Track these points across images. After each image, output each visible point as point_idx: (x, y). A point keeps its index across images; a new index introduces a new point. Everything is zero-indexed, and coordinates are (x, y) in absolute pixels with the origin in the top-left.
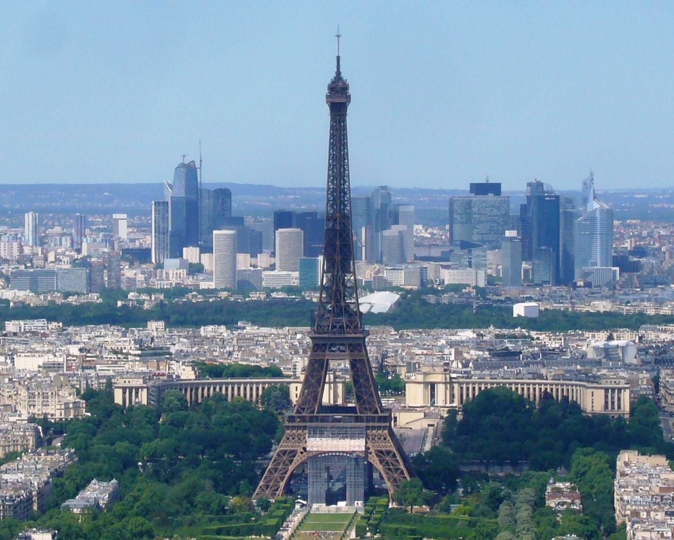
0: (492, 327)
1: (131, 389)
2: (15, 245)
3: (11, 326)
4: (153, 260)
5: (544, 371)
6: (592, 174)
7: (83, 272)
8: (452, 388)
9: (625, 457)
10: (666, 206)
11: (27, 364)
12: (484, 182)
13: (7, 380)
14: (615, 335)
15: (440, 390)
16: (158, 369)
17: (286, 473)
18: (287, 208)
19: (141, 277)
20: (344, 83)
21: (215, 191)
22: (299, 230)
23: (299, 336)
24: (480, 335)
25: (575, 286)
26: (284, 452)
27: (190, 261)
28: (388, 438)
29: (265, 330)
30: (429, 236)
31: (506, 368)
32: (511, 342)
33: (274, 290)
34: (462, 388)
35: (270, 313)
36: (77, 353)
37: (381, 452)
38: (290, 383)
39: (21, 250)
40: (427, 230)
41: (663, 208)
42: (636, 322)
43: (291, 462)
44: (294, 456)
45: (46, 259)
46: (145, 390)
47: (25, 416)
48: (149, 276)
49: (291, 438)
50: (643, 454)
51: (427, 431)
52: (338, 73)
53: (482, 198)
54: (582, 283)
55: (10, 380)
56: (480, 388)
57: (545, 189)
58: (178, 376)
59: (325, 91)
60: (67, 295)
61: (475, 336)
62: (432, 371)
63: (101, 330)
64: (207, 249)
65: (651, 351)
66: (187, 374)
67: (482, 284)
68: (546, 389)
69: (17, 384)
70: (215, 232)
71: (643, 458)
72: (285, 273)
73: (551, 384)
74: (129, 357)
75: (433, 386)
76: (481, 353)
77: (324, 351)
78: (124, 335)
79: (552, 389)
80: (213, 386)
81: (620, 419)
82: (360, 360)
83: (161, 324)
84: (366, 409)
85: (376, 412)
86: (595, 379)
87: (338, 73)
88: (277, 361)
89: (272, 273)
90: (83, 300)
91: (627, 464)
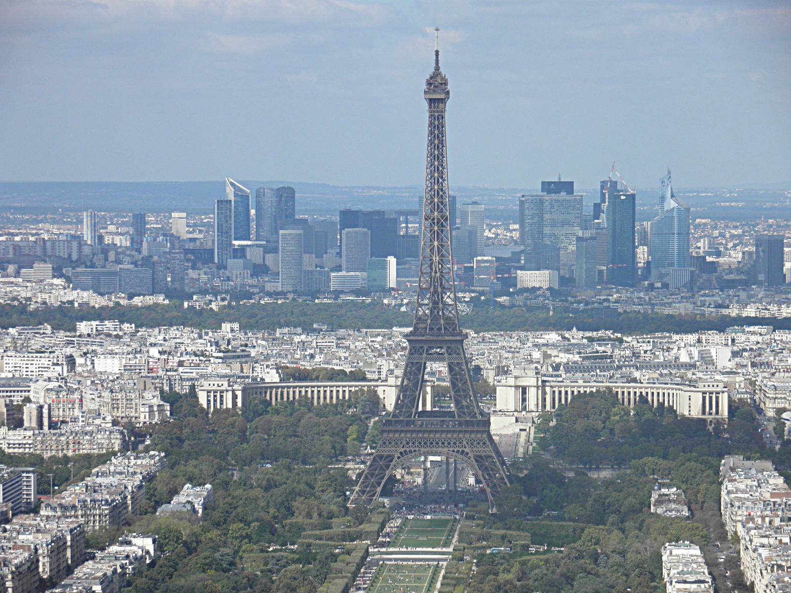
0: (574, 329)
1: (215, 392)
2: (75, 244)
3: (83, 327)
4: (216, 261)
5: (637, 374)
6: (669, 173)
8: (544, 393)
9: (728, 461)
10: (733, 204)
11: (109, 365)
12: (557, 180)
13: (89, 382)
14: (704, 337)
15: (532, 394)
16: (242, 371)
17: (383, 478)
18: (355, 208)
20: (443, 78)
21: (278, 189)
22: (366, 230)
23: (379, 339)
24: (564, 338)
25: (651, 287)
26: (381, 457)
27: (254, 262)
28: (488, 443)
30: (493, 236)
31: (598, 371)
32: (600, 345)
33: (342, 292)
34: (554, 392)
36: (158, 355)
37: (481, 457)
38: (377, 386)
40: (490, 231)
41: (731, 206)
42: (722, 325)
43: (388, 467)
44: (391, 461)
45: (106, 259)
46: (230, 393)
47: (109, 419)
49: (387, 443)
50: (748, 459)
51: (518, 436)
52: (437, 68)
53: (554, 196)
54: (659, 285)
55: (93, 382)
56: (573, 392)
57: (619, 188)
58: (262, 379)
59: (424, 87)
60: (131, 297)
61: (560, 338)
62: (524, 375)
63: (173, 332)
64: (275, 250)
65: (746, 354)
66: (272, 377)
68: (641, 393)
69: (99, 387)
70: (281, 232)
71: (748, 463)
72: (352, 273)
73: (646, 388)
74: (212, 359)
75: (524, 390)
76: (571, 356)
77: (421, 354)
78: (200, 337)
79: (647, 393)
80: (297, 390)
81: (718, 423)
82: (458, 363)
83: (236, 326)
84: (464, 413)
85: (474, 416)
86: (692, 383)
87: (437, 68)
88: (361, 364)
89: (340, 274)
91: (733, 469)
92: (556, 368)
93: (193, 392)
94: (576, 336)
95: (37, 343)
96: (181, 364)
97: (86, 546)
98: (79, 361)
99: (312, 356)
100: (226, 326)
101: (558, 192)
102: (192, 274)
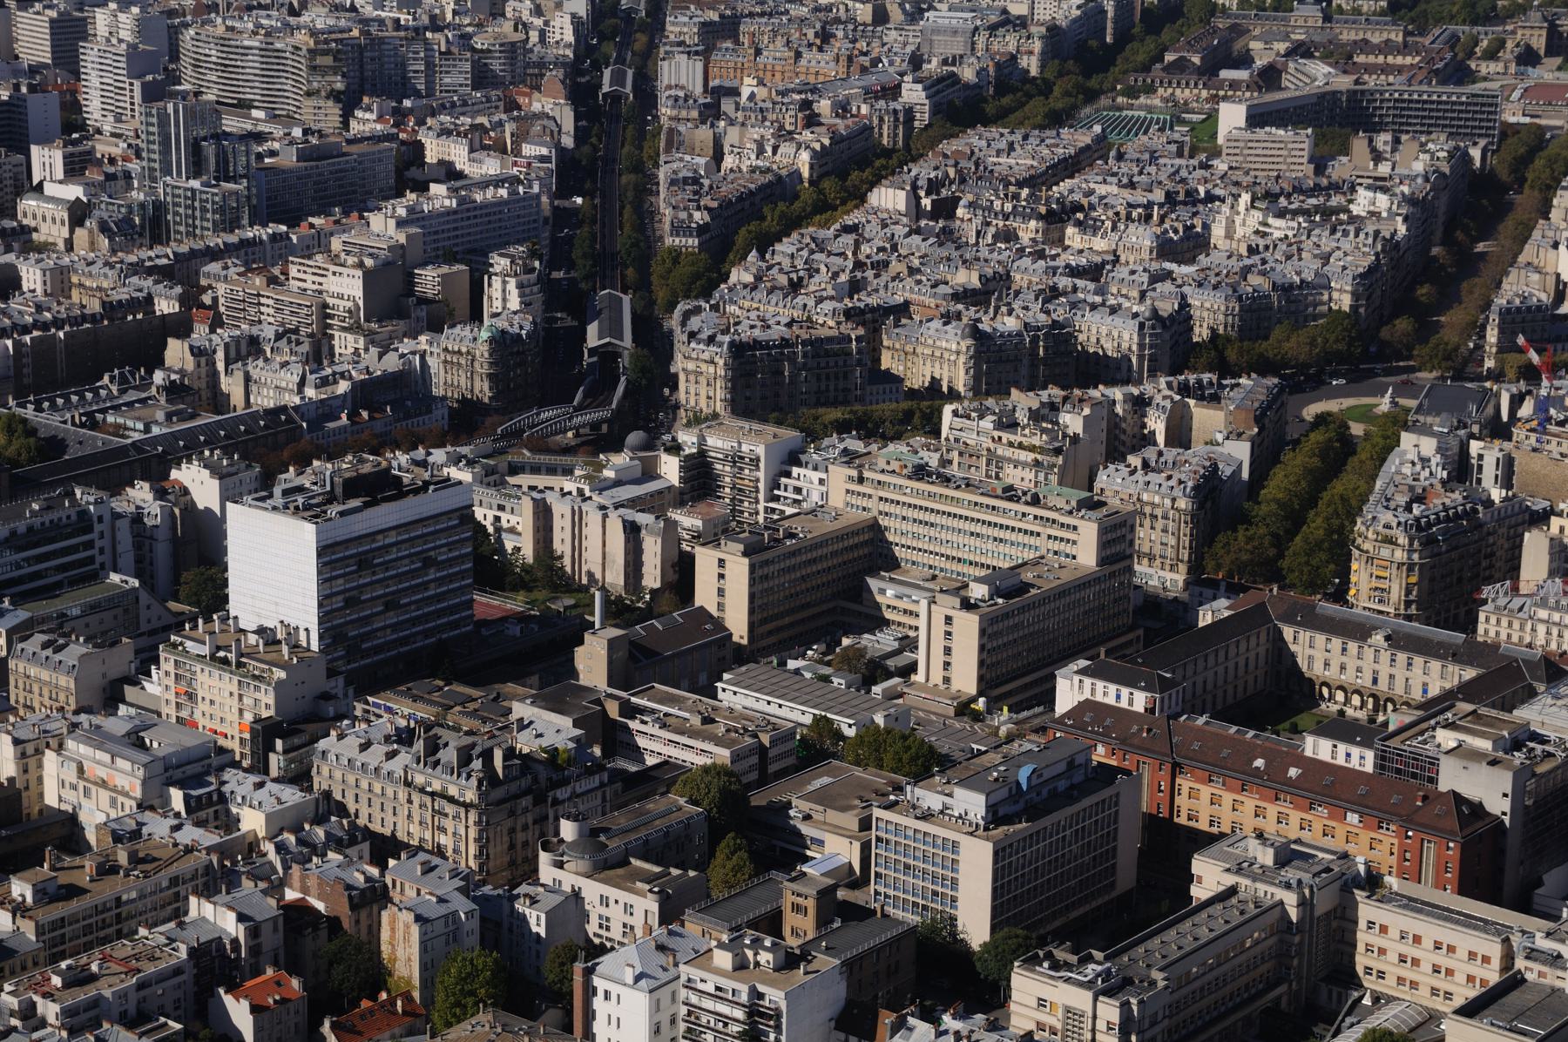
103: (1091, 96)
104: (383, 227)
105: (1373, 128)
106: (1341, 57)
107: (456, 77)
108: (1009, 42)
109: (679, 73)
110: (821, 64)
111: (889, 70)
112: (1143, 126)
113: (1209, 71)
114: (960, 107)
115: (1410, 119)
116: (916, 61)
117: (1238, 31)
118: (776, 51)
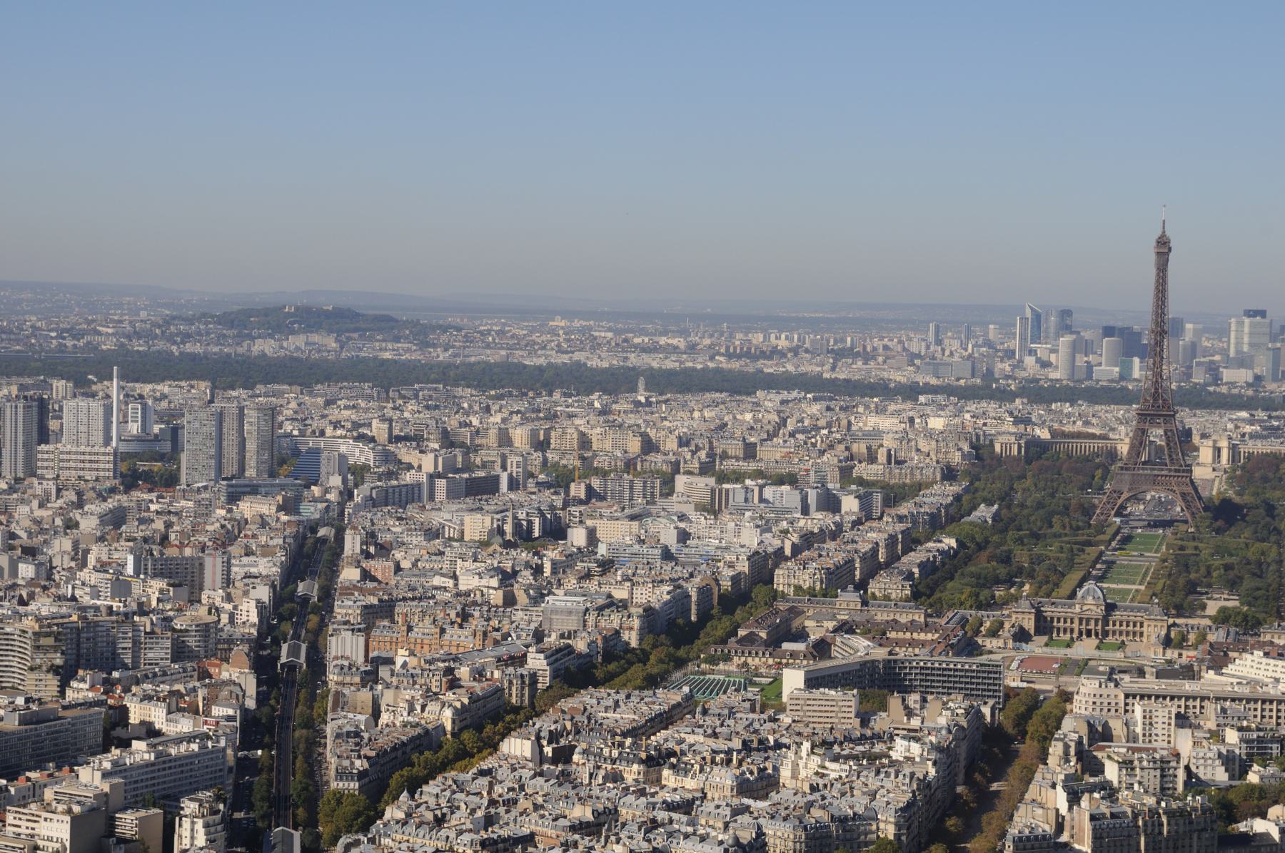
2: (923, 344)
3: (922, 399)
7: (969, 364)
11: (937, 423)
15: (1225, 454)
18: (1112, 323)
19: (1008, 368)
24: (1252, 415)
29: (1098, 408)
35: (1100, 395)
39: (928, 347)
48: (1014, 367)
59: (1154, 244)
60: (958, 379)
66: (1044, 434)
67: (1250, 380)
75: (1219, 450)
83: (1025, 400)
90: (969, 383)
92: (1243, 435)
93: (992, 445)
94: (1261, 415)
95: (892, 407)
96: (985, 424)
97: (911, 542)
98: (917, 420)
99: (1074, 422)
100: (1018, 401)
101: (1254, 316)
102: (1000, 366)
103: (680, 663)
104: (91, 778)
105: (905, 690)
106: (879, 634)
107: (159, 652)
108: (613, 620)
109: (344, 647)
110: (461, 638)
111: (516, 644)
112: (722, 688)
113: (774, 643)
114: (575, 673)
115: (935, 683)
116: (539, 636)
117: (795, 612)
118: (424, 628)
